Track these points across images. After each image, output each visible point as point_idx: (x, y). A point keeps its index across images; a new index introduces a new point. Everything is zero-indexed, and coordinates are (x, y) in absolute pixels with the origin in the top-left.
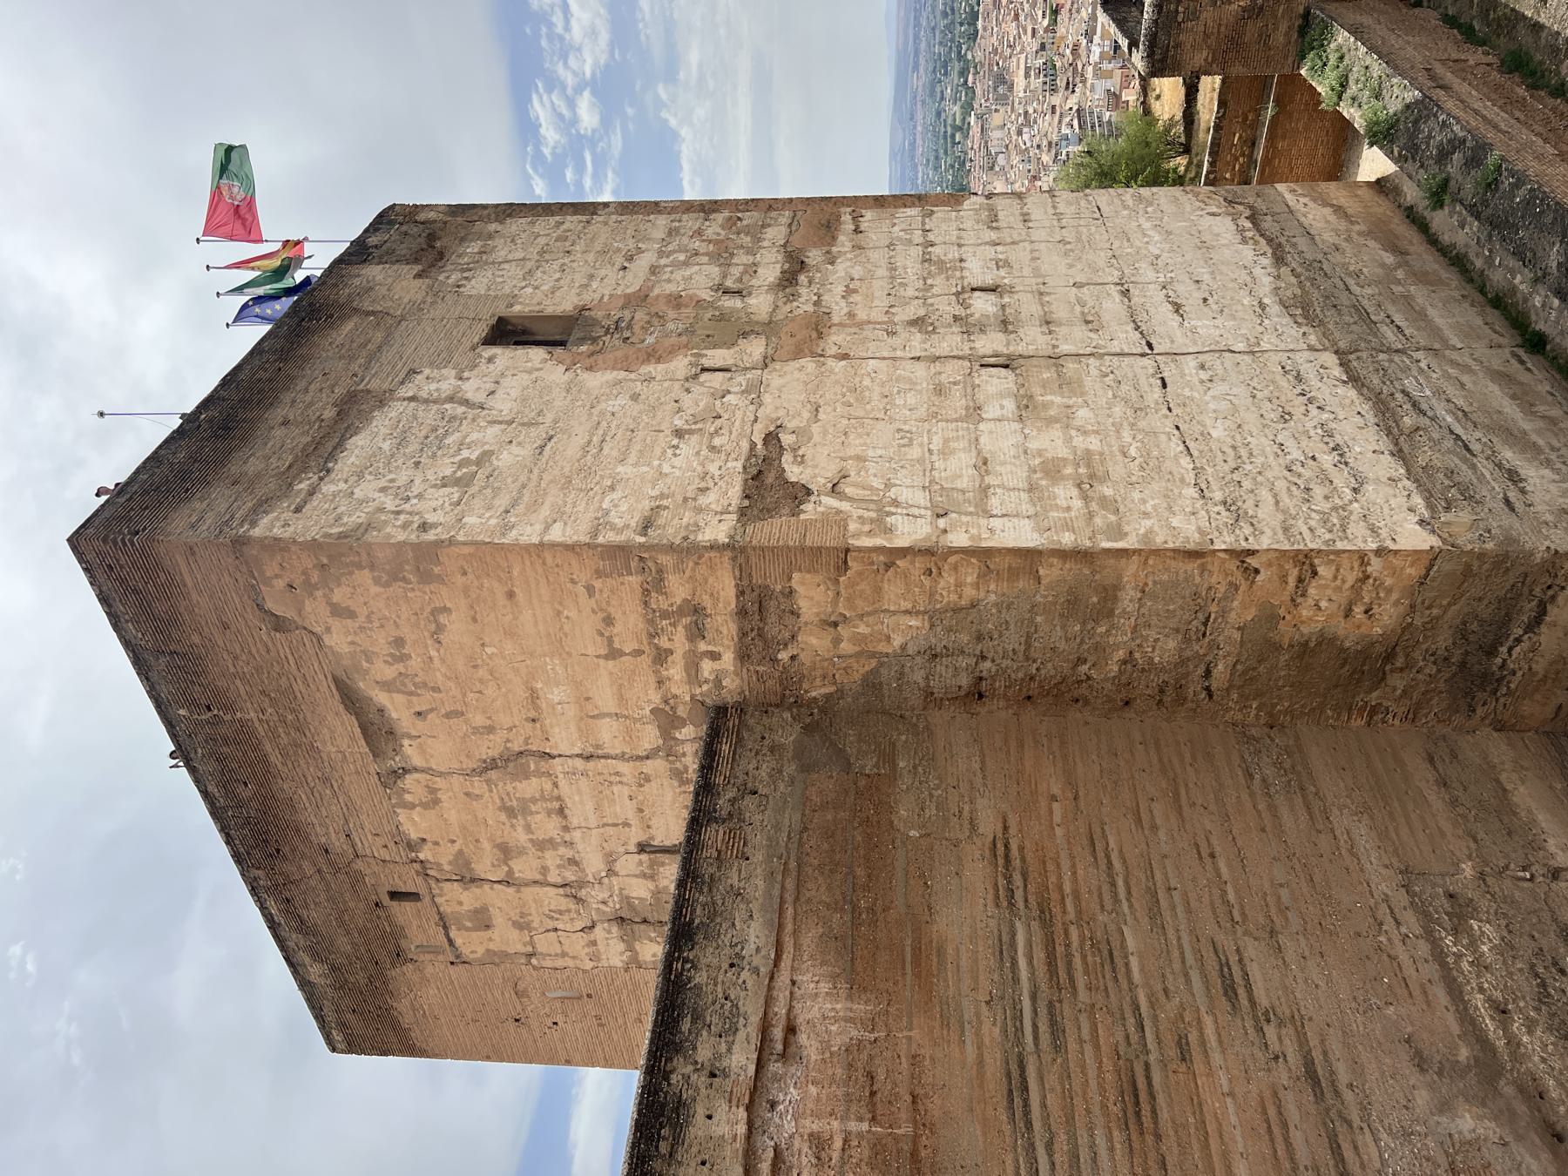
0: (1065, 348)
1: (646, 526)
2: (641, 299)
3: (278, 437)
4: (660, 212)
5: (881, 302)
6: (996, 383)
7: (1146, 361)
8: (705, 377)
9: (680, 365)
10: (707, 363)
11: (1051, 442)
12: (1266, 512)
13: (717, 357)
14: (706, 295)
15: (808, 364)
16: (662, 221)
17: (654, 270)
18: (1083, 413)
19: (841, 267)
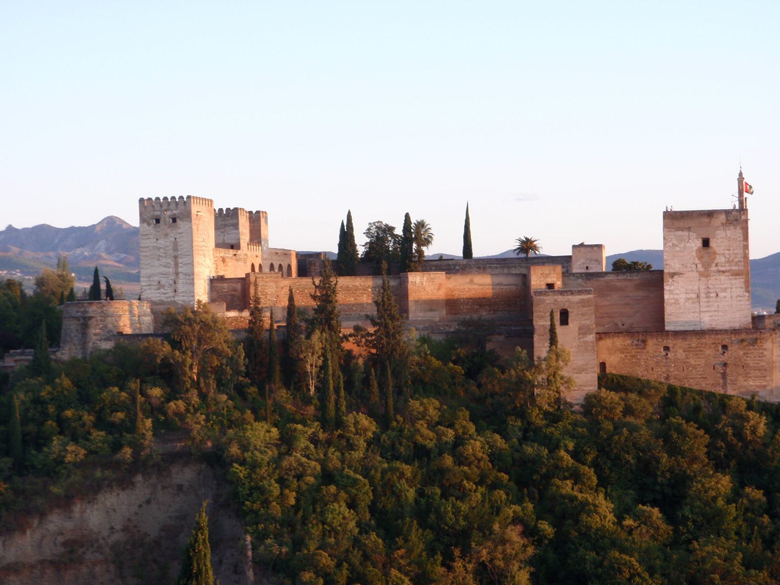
0: (701, 303)
1: (667, 264)
2: (715, 253)
3: (681, 224)
4: (744, 250)
5: (714, 283)
6: (694, 296)
7: (698, 311)
8: (695, 266)
9: (697, 261)
10: (698, 266)
11: (682, 301)
12: (670, 317)
13: (700, 266)
14: (716, 262)
15: (698, 276)
16: (741, 251)
17: (724, 254)
18: (687, 304)
19: (724, 278)
